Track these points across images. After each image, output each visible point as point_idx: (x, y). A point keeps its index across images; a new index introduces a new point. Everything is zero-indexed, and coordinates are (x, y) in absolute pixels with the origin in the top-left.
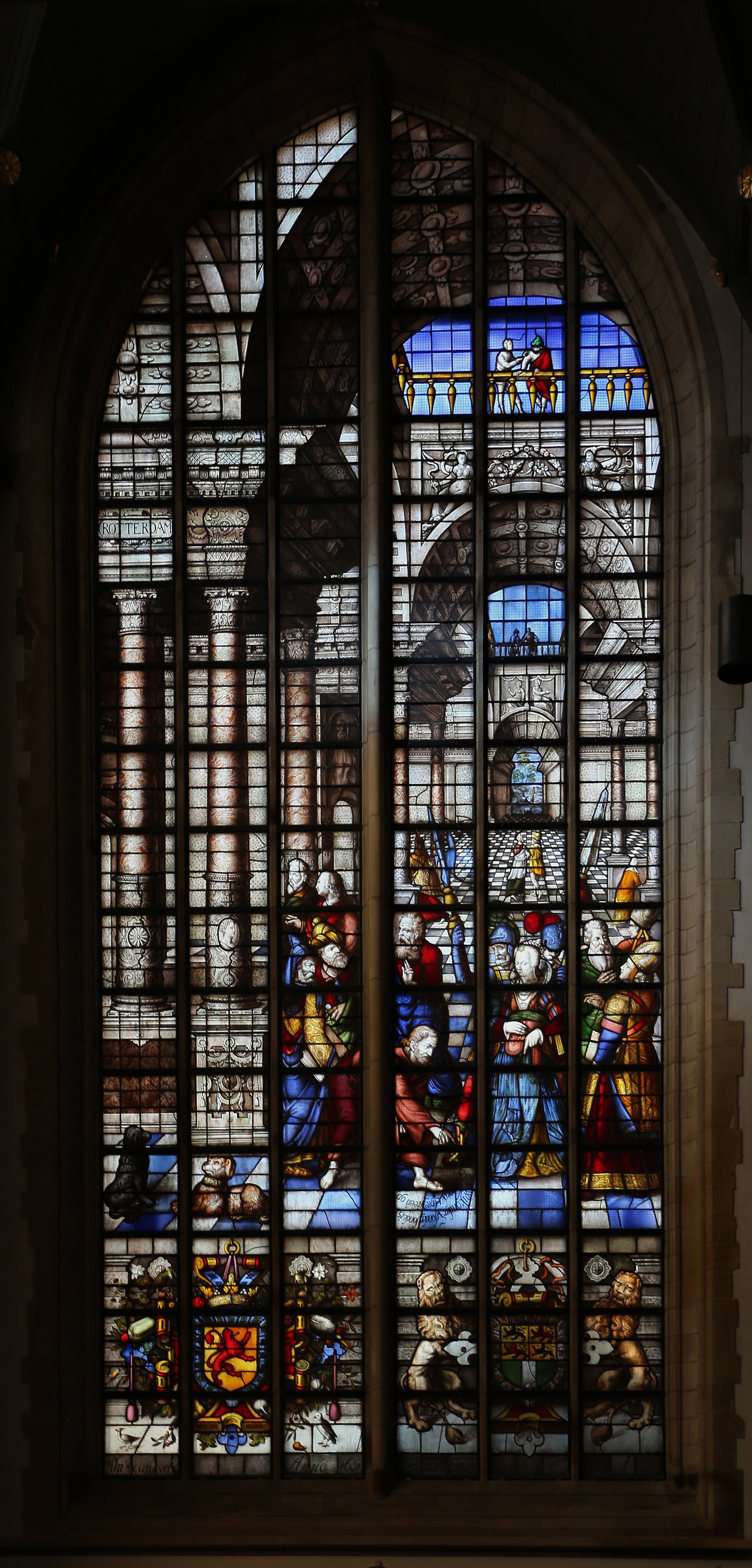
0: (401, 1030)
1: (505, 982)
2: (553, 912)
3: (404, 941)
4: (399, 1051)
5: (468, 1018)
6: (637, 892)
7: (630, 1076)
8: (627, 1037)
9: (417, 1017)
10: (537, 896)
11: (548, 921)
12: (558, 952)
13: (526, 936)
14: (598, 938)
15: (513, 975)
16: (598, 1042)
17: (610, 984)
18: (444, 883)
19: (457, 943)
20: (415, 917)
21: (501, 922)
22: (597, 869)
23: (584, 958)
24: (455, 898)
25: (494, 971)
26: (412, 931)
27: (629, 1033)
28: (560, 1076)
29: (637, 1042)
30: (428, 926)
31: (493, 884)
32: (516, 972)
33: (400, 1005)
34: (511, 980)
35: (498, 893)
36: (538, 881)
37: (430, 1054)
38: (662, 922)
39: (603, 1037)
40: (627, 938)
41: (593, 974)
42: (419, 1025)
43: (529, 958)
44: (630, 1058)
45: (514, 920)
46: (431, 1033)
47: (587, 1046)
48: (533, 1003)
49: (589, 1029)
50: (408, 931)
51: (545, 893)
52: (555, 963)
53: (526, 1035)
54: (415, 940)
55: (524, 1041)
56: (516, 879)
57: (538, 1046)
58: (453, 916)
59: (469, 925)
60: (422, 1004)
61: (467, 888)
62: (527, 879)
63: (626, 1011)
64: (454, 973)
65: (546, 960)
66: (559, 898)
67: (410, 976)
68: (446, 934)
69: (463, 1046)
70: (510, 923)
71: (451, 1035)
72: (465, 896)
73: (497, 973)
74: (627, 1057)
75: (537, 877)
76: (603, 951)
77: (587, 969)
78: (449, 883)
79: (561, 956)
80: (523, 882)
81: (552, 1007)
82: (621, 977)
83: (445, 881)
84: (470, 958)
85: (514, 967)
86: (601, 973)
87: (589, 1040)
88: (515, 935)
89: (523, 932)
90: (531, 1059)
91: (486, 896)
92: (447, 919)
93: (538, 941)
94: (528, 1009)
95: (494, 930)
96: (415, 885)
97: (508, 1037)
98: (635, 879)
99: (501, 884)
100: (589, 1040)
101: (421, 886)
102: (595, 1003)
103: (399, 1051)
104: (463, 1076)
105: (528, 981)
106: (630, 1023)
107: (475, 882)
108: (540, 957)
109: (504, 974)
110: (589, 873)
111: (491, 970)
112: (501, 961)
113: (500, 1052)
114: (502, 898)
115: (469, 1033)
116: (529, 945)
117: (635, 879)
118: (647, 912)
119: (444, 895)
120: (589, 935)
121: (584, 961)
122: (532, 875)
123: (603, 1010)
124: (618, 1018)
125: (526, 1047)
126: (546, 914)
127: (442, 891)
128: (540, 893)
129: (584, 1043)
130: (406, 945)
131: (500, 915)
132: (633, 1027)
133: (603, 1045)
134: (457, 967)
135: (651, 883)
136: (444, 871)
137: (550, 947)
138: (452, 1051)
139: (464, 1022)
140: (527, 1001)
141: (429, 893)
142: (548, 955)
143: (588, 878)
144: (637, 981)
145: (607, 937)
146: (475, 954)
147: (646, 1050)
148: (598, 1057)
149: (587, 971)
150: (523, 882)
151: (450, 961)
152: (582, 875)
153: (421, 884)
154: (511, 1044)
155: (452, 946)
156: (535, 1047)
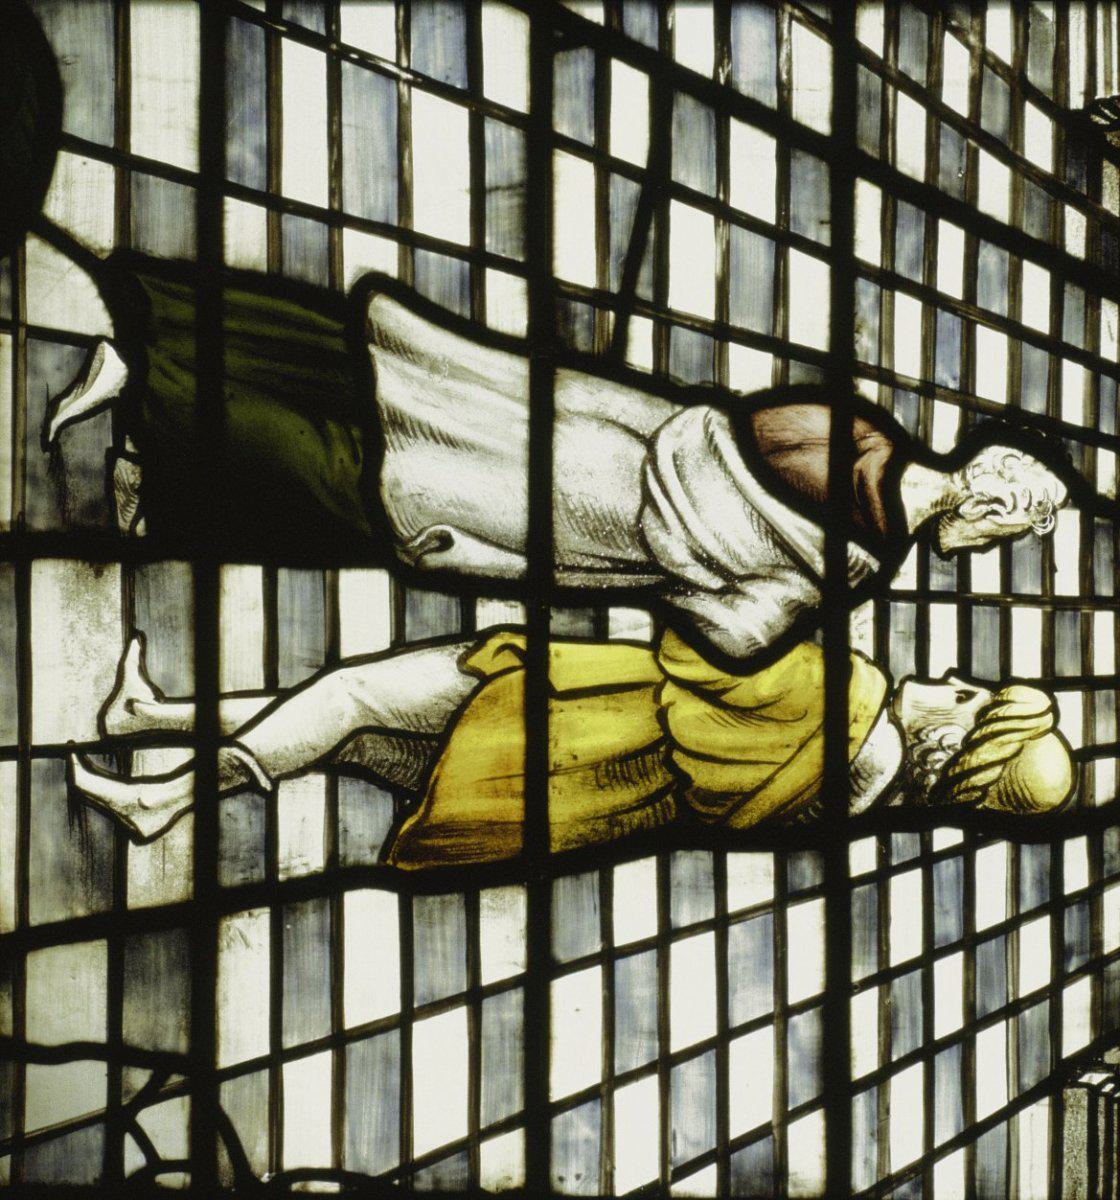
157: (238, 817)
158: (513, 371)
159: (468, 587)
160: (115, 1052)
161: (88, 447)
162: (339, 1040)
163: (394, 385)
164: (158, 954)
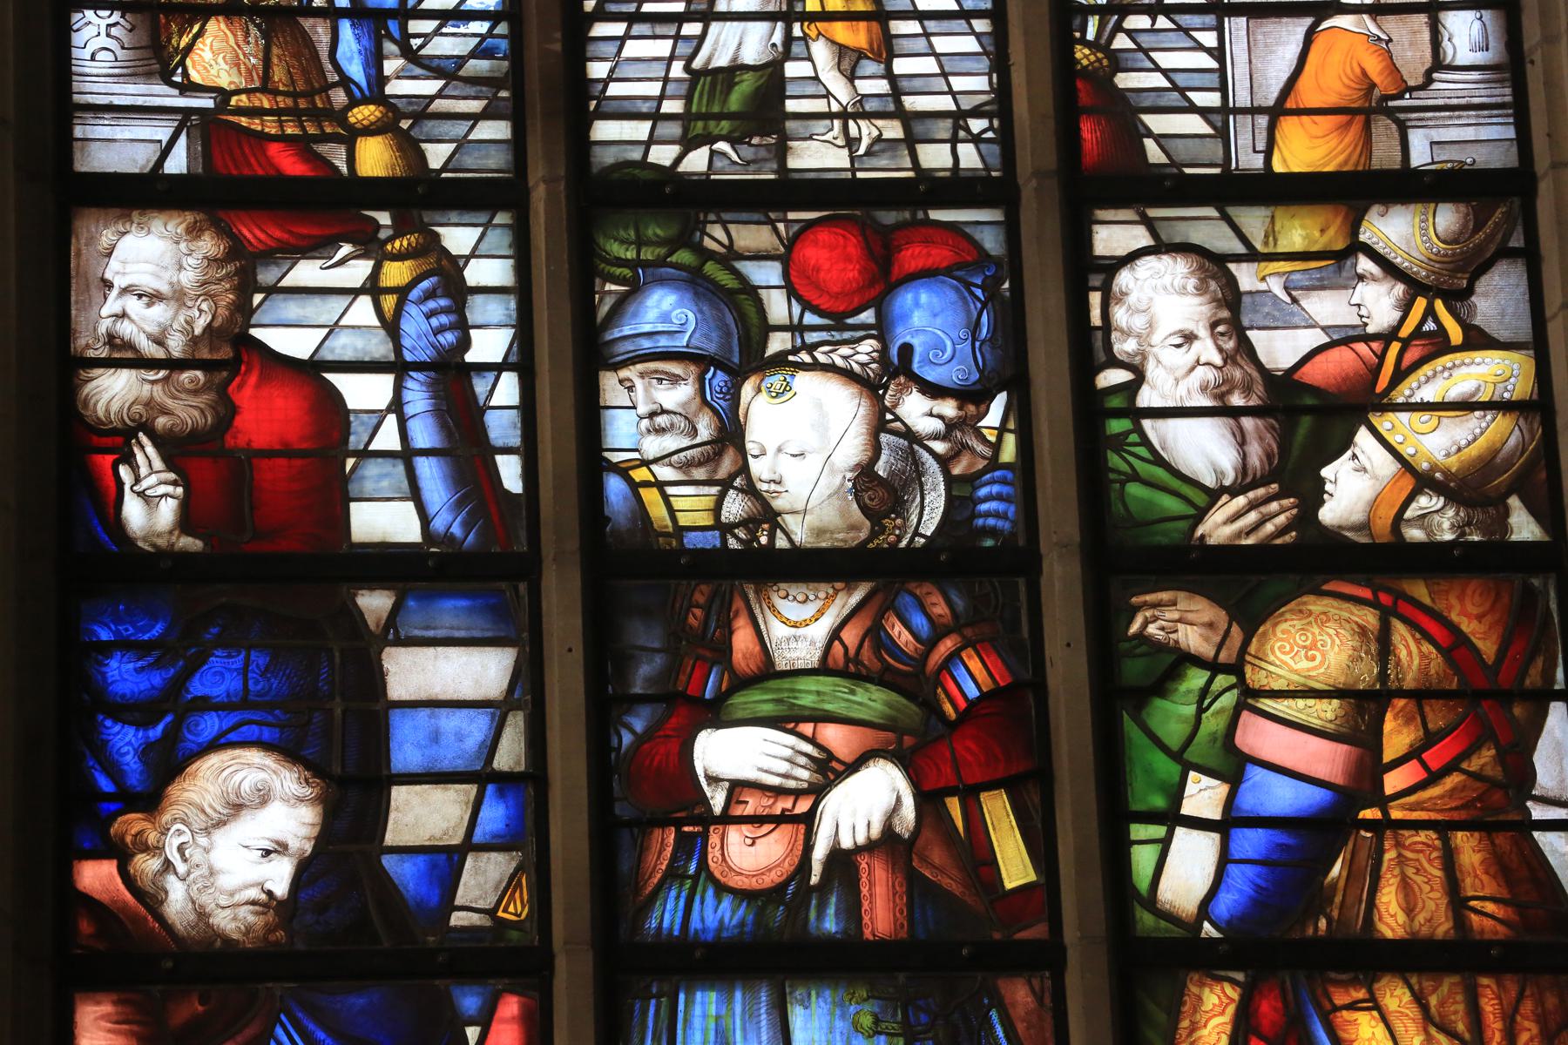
0: (114, 770)
1: (693, 540)
2: (937, 215)
3: (129, 345)
4: (96, 876)
5: (498, 709)
6: (1384, 131)
7: (1419, 999)
8: (1383, 802)
9: (205, 705)
10: (851, 143)
11: (912, 257)
12: (973, 396)
13: (797, 328)
14: (1189, 338)
15: (735, 507)
16: (1226, 825)
17: (1263, 548)
18: (345, 81)
19: (424, 355)
20: (194, 232)
21: (661, 262)
22: (1162, 22)
23: (1117, 426)
24: (410, 148)
25: (635, 486)
26: (178, 297)
27: (1393, 782)
28: (1020, 994)
29: (1443, 828)
30: (267, 276)
31: (614, 89)
32: (750, 490)
33: (106, 649)
34: (726, 529)
35: (641, 130)
36: (851, 78)
37: (281, 888)
38: (1531, 258)
39: (1249, 801)
40: (1346, 338)
41: (1171, 504)
42: (215, 745)
43: (822, 427)
44: (1410, 911)
45: (730, 256)
46: (286, 780)
47: (1166, 843)
48: (851, 636)
49: (1167, 768)
50: (154, 297)
51: (893, 130)
52: (959, 450)
53: (818, 791)
54: (194, 341)
55: (808, 820)
56: (736, 69)
57: (887, 843)
58: (399, 230)
59: (489, 271)
60: (229, 644)
61: (475, 106)
62: (792, 69)
63: (1366, 673)
64: (415, 494)
65: (910, 435)
66: (969, 156)
67: (167, 512)
68: (363, 311)
69: (470, 845)
70: (710, 268)
71: (399, 794)
72: (462, 143)
73: (650, 496)
74: (1389, 899)
75: (849, 62)
76: (1221, 391)
77: (1135, 477)
78: (379, 80)
79: (994, 414)
80: (771, 81)
81: (954, 656)
82: (1329, 514)
83: (356, 70)
84: (502, 426)
85: (744, 469)
86: (1214, 495)
87: (1173, 818)
88: (741, 318)
89: (778, 307)
90: (852, 910)
91: (581, 144)
92: (369, 244)
93: (868, 346)
94: (824, 668)
95: (622, 302)
96: (188, 88)
97: (718, 800)
98: (1374, 67)
99: (654, 89)
100: (1173, 818)
101: (223, 95)
102: (1192, 639)
103: (96, 876)
104: (470, 1002)
105: (820, 532)
106: (1397, 737)
107: (516, 77)
108: (881, 422)
109: (692, 504)
110: (1122, 42)
111: (614, 486)
112: (670, 443)
113: (674, 874)
114: (663, 155)
115: (505, 781)
116: (815, 366)
117: (1374, 67)
118: (1447, 218)
119: (351, 137)
120: (1138, 323)
121: (1119, 442)
122: (820, 50)
123: (1236, 668)
124: (1324, 712)
125: (820, 852)
126: (899, 226)
127: (340, 117)
128: (866, 131)
129: (1139, 831)
130: (141, 362)
131: (654, 231)
132: (1413, 754)
133: (1250, 842)
134: (427, 469)
135: (1447, 87)
136: (346, 28)
137: (931, 375)
138: (402, 871)
139: (476, 727)
140: (820, 631)
141: (272, 129)
142: (915, 410)
143: (1117, 62)
144: (1415, 534)
145: (1239, 331)
146: (527, 407)
147: (1499, 865)
148: (1226, 903)
149: (1134, 489)
150: (771, 81)
151: (388, 438)
152: (1081, 53)
153: (224, 77)
154: (735, 836)
155: (398, 367)
156: (870, 847)
157: (870, 106)
158: (715, 27)
159: (789, 39)
160: (954, 141)
161: (747, 152)
162: (944, 75)
163: (722, 61)
164: (919, 128)
